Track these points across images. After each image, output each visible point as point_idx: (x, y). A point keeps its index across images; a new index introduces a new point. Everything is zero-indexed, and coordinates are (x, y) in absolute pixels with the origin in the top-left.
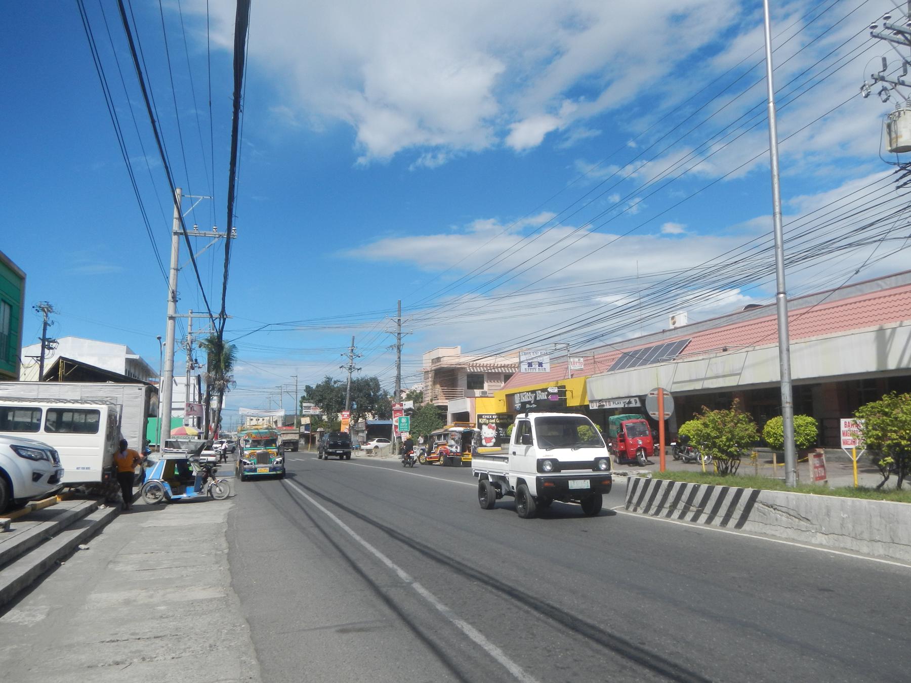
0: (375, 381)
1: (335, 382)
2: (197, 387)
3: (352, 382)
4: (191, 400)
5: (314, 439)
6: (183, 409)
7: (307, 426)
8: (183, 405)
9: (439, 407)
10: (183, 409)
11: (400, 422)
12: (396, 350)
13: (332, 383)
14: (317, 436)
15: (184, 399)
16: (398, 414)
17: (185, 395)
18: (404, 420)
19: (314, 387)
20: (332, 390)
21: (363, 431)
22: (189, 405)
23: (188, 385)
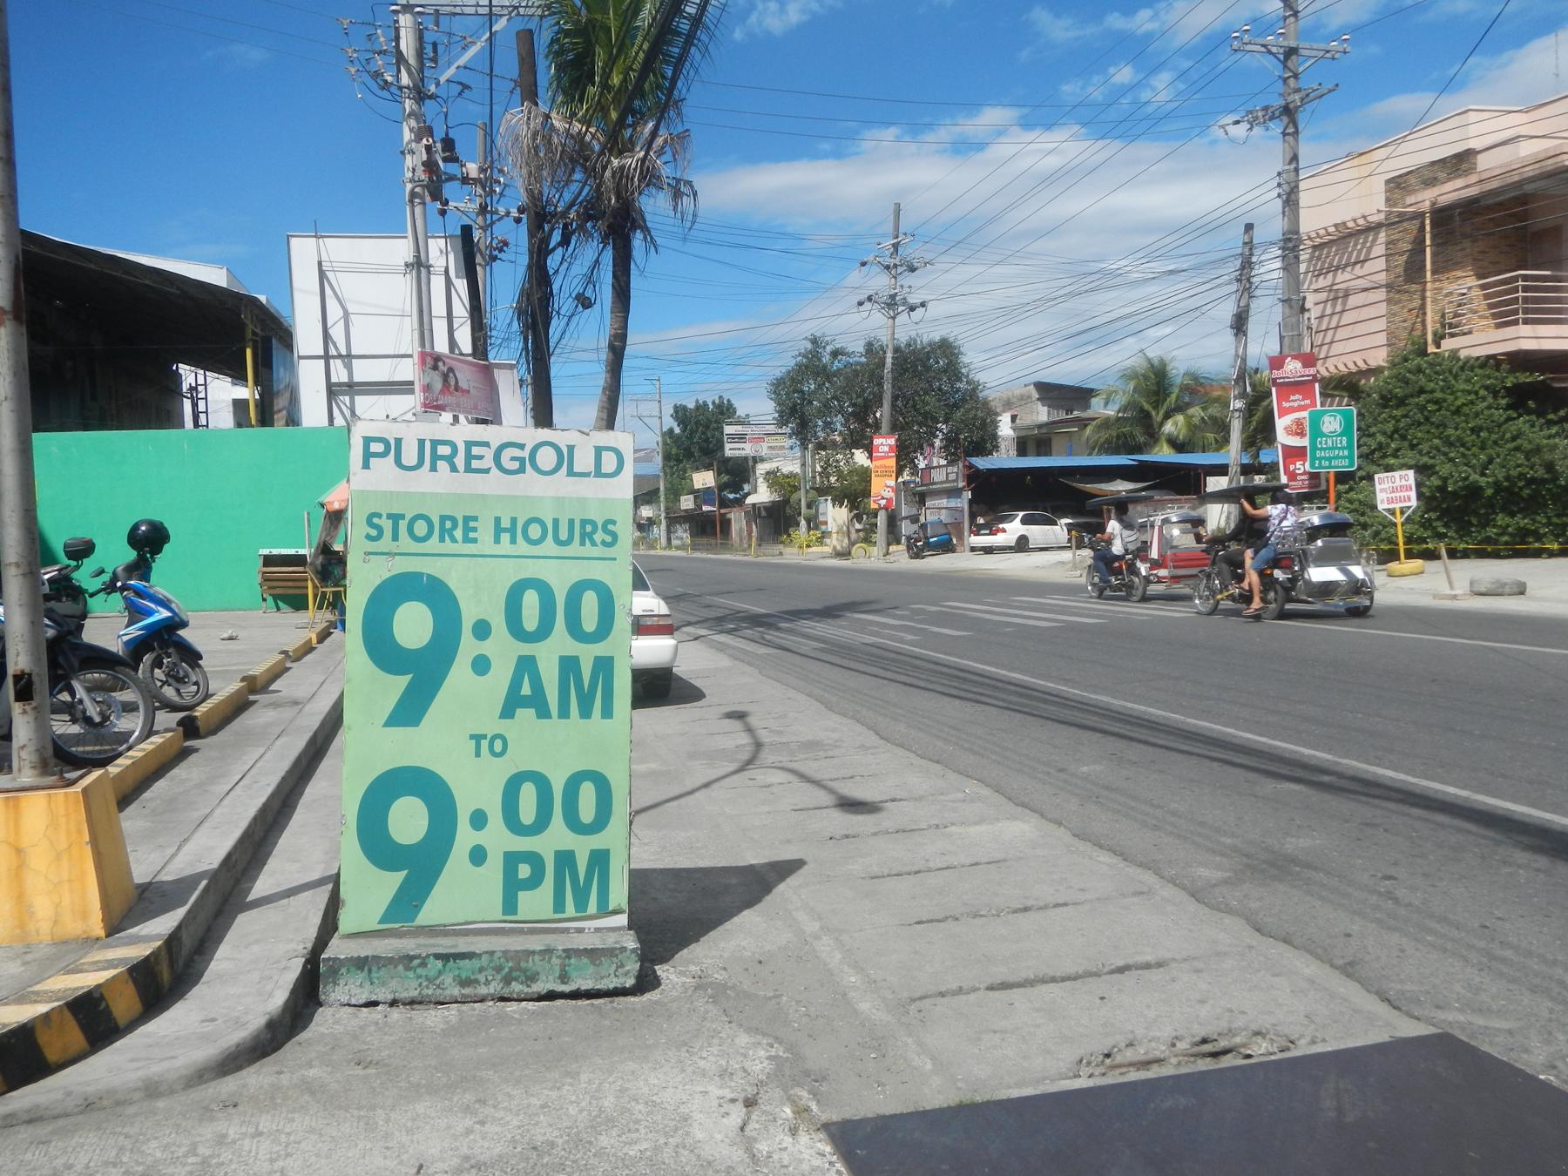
0: (946, 349)
1: (835, 354)
2: (461, 285)
3: (897, 350)
4: (441, 346)
5: (726, 524)
6: (404, 387)
7: (702, 495)
8: (407, 370)
9: (1521, 360)
10: (404, 387)
11: (1317, 432)
12: (1276, 128)
13: (826, 359)
14: (737, 519)
15: (408, 341)
16: (1296, 399)
17: (410, 324)
18: (1331, 424)
19: (691, 405)
20: (822, 373)
21: (954, 493)
22: (431, 361)
23: (419, 265)
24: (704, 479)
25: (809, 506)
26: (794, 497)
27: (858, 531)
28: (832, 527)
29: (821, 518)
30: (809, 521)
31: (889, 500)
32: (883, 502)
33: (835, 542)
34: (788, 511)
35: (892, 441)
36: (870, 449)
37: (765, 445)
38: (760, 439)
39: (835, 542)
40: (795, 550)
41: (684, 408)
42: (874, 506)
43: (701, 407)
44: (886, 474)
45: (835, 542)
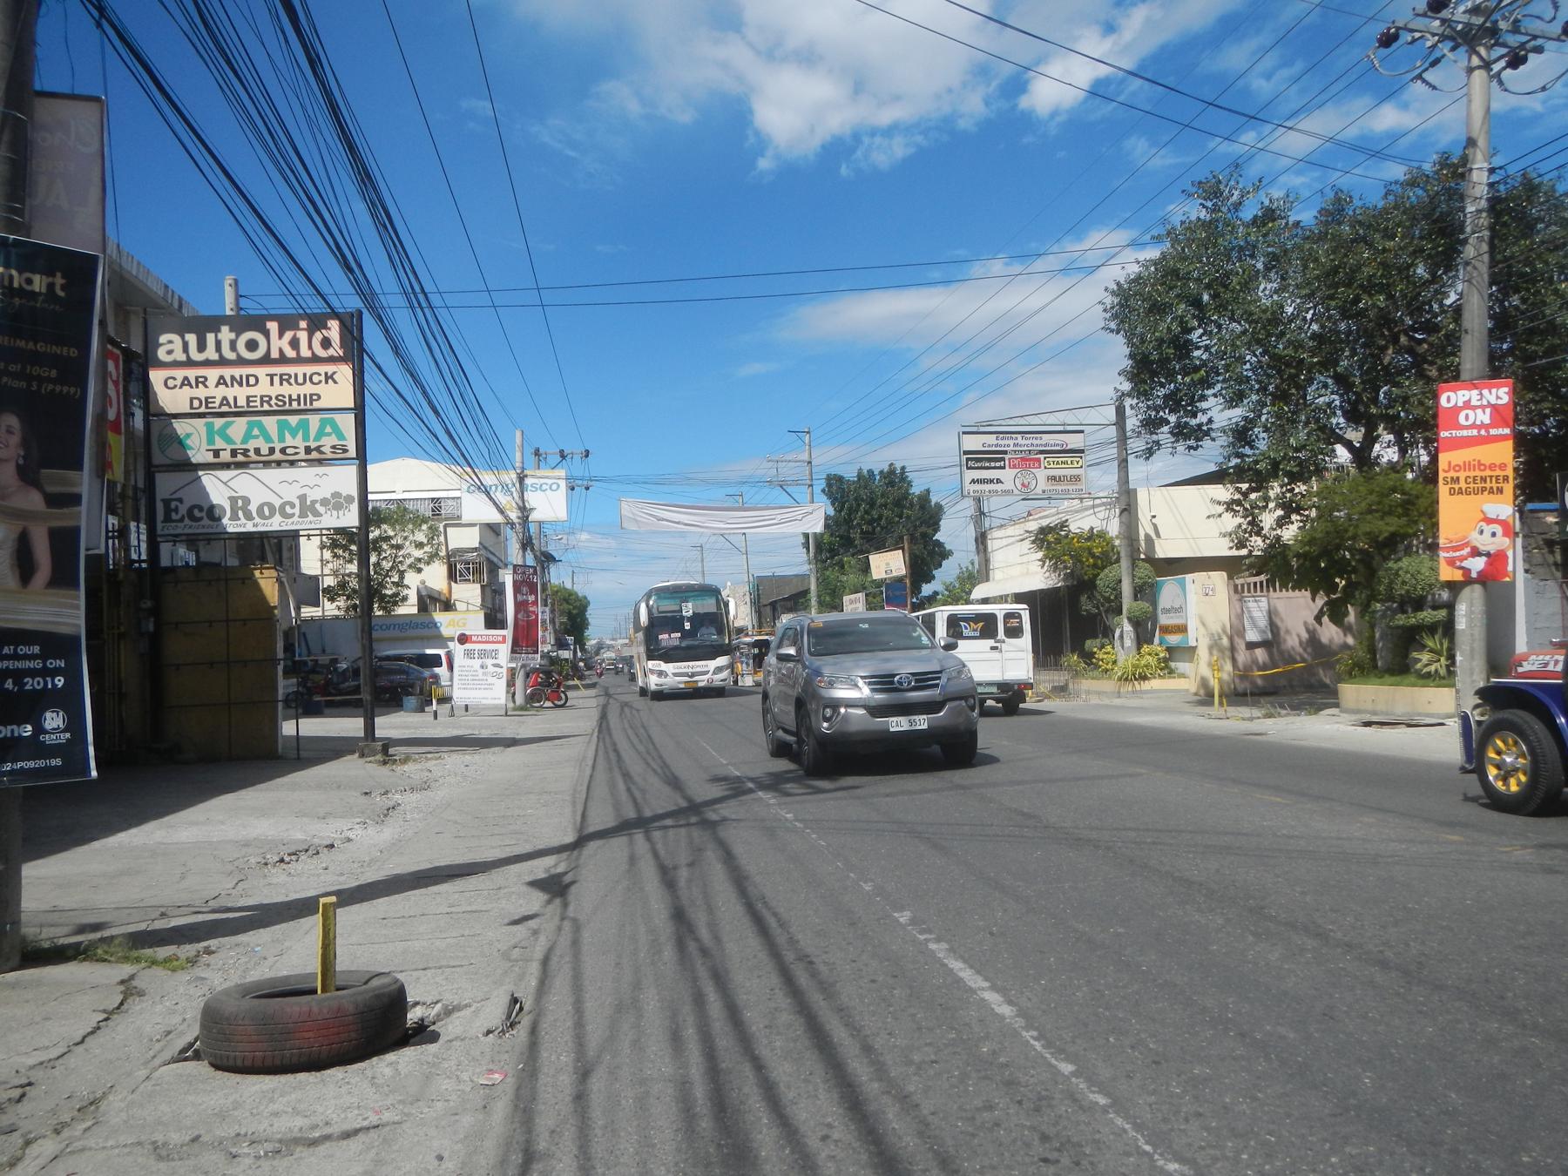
24: (888, 564)
25: (1140, 591)
26: (1105, 577)
27: (1251, 646)
28: (1196, 636)
29: (1164, 620)
30: (1137, 623)
31: (1496, 559)
32: (1477, 565)
33: (1202, 669)
34: (1086, 605)
35: (1501, 394)
36: (1422, 426)
37: (1041, 474)
38: (1028, 461)
39: (1205, 671)
40: (1108, 685)
41: (840, 479)
42: (1447, 573)
43: (865, 479)
44: (1484, 486)
45: (1205, 671)
